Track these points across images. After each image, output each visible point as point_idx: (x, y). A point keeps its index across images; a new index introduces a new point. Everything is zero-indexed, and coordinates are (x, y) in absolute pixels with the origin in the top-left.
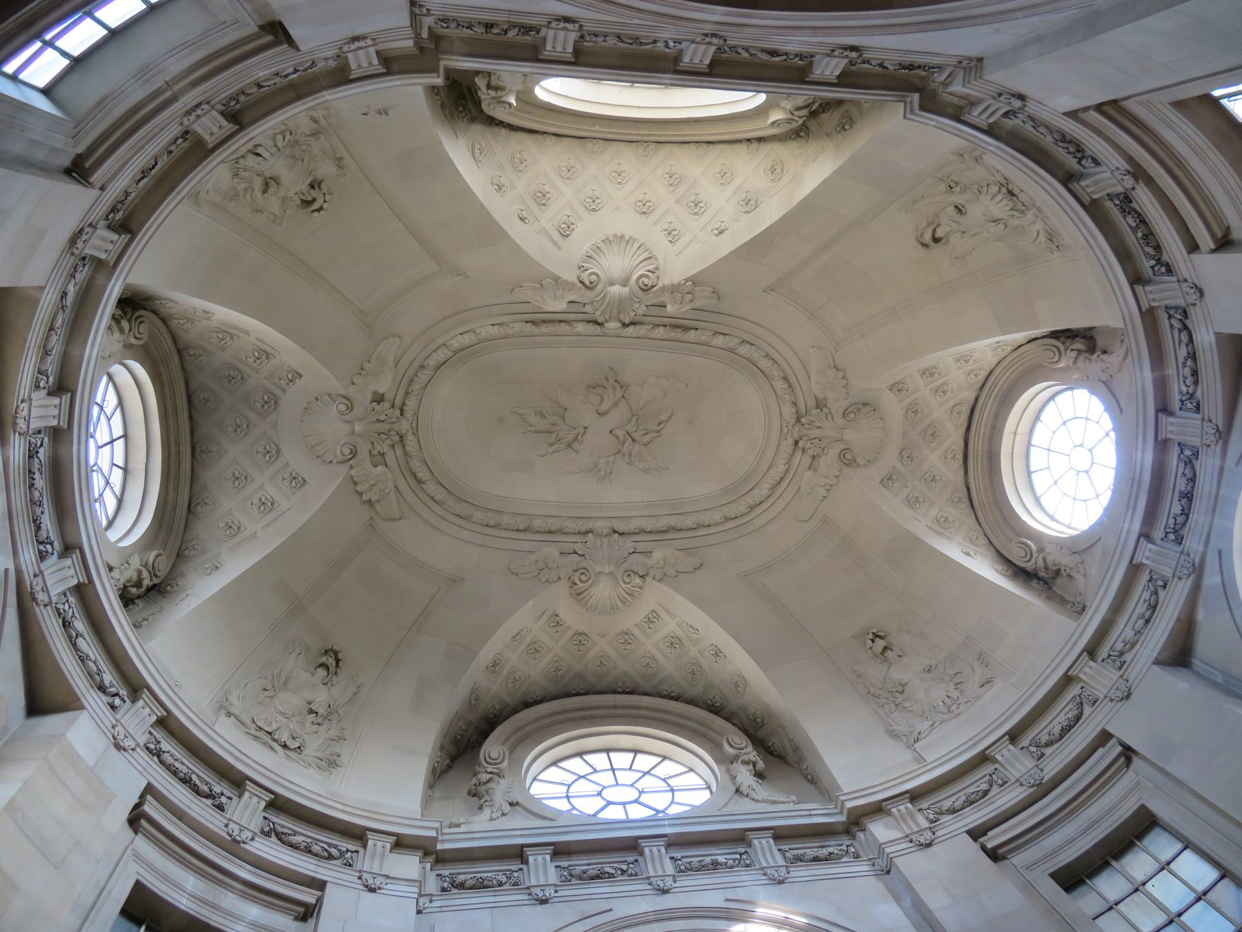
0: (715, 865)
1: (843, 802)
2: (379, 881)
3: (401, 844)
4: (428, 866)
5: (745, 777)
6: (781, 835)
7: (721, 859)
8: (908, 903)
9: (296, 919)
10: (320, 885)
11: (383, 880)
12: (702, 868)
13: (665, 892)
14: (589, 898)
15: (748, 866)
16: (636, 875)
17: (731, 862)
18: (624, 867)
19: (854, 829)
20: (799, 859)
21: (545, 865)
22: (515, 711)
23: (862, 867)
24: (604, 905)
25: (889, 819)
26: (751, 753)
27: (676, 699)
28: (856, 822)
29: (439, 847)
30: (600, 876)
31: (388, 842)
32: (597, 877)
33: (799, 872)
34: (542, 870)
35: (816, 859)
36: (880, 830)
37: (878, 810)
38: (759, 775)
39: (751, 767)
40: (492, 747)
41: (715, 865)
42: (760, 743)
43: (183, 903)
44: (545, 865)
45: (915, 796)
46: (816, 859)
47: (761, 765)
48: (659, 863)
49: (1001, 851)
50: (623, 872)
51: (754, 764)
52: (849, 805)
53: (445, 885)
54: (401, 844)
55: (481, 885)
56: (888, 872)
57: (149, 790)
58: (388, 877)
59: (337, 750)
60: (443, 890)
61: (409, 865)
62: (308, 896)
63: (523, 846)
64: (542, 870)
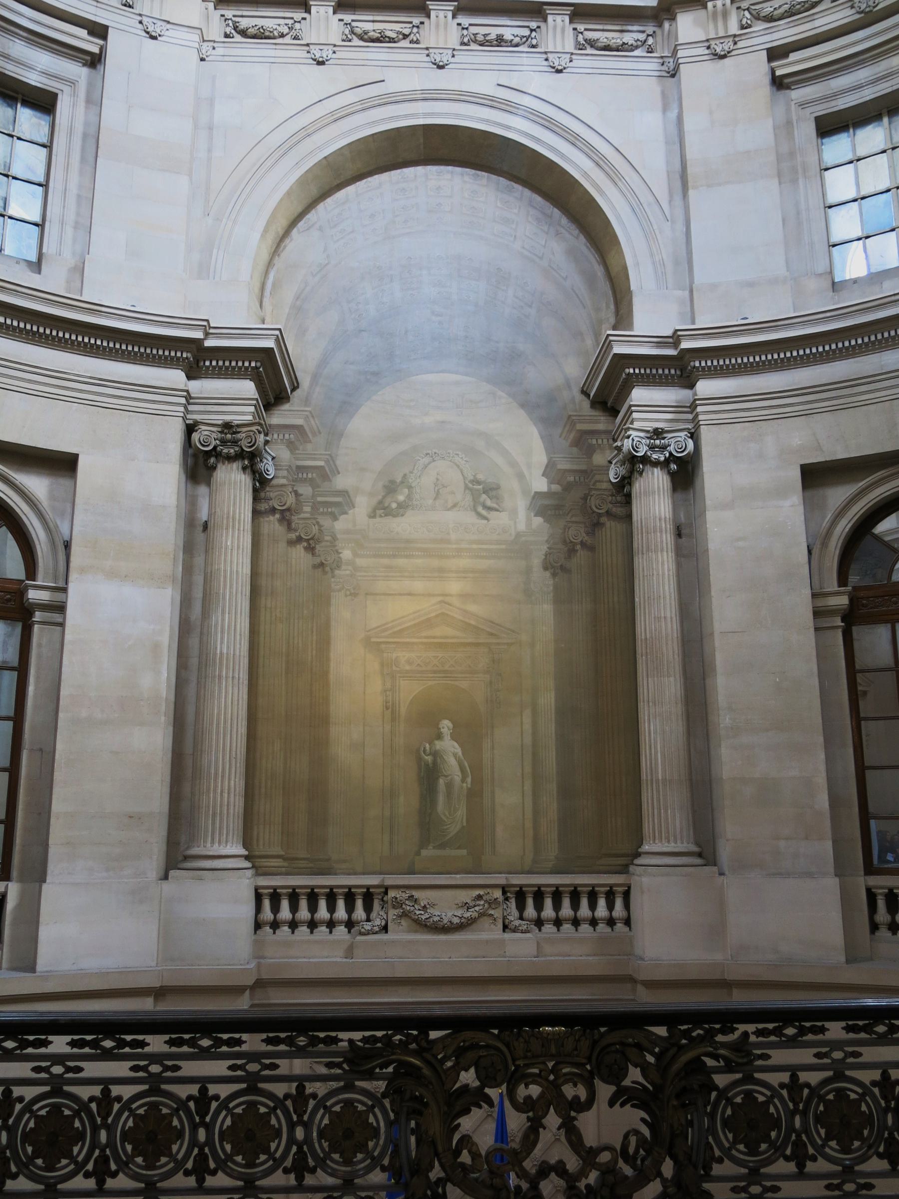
0: (500, 41)
7: (508, 33)
12: (485, 43)
15: (533, 46)
16: (417, 42)
17: (517, 40)
18: (406, 31)
20: (592, 43)
23: (652, 65)
30: (381, 39)
33: (586, 62)
35: (607, 48)
41: (500, 41)
46: (607, 48)
50: (405, 36)
62: (92, 46)
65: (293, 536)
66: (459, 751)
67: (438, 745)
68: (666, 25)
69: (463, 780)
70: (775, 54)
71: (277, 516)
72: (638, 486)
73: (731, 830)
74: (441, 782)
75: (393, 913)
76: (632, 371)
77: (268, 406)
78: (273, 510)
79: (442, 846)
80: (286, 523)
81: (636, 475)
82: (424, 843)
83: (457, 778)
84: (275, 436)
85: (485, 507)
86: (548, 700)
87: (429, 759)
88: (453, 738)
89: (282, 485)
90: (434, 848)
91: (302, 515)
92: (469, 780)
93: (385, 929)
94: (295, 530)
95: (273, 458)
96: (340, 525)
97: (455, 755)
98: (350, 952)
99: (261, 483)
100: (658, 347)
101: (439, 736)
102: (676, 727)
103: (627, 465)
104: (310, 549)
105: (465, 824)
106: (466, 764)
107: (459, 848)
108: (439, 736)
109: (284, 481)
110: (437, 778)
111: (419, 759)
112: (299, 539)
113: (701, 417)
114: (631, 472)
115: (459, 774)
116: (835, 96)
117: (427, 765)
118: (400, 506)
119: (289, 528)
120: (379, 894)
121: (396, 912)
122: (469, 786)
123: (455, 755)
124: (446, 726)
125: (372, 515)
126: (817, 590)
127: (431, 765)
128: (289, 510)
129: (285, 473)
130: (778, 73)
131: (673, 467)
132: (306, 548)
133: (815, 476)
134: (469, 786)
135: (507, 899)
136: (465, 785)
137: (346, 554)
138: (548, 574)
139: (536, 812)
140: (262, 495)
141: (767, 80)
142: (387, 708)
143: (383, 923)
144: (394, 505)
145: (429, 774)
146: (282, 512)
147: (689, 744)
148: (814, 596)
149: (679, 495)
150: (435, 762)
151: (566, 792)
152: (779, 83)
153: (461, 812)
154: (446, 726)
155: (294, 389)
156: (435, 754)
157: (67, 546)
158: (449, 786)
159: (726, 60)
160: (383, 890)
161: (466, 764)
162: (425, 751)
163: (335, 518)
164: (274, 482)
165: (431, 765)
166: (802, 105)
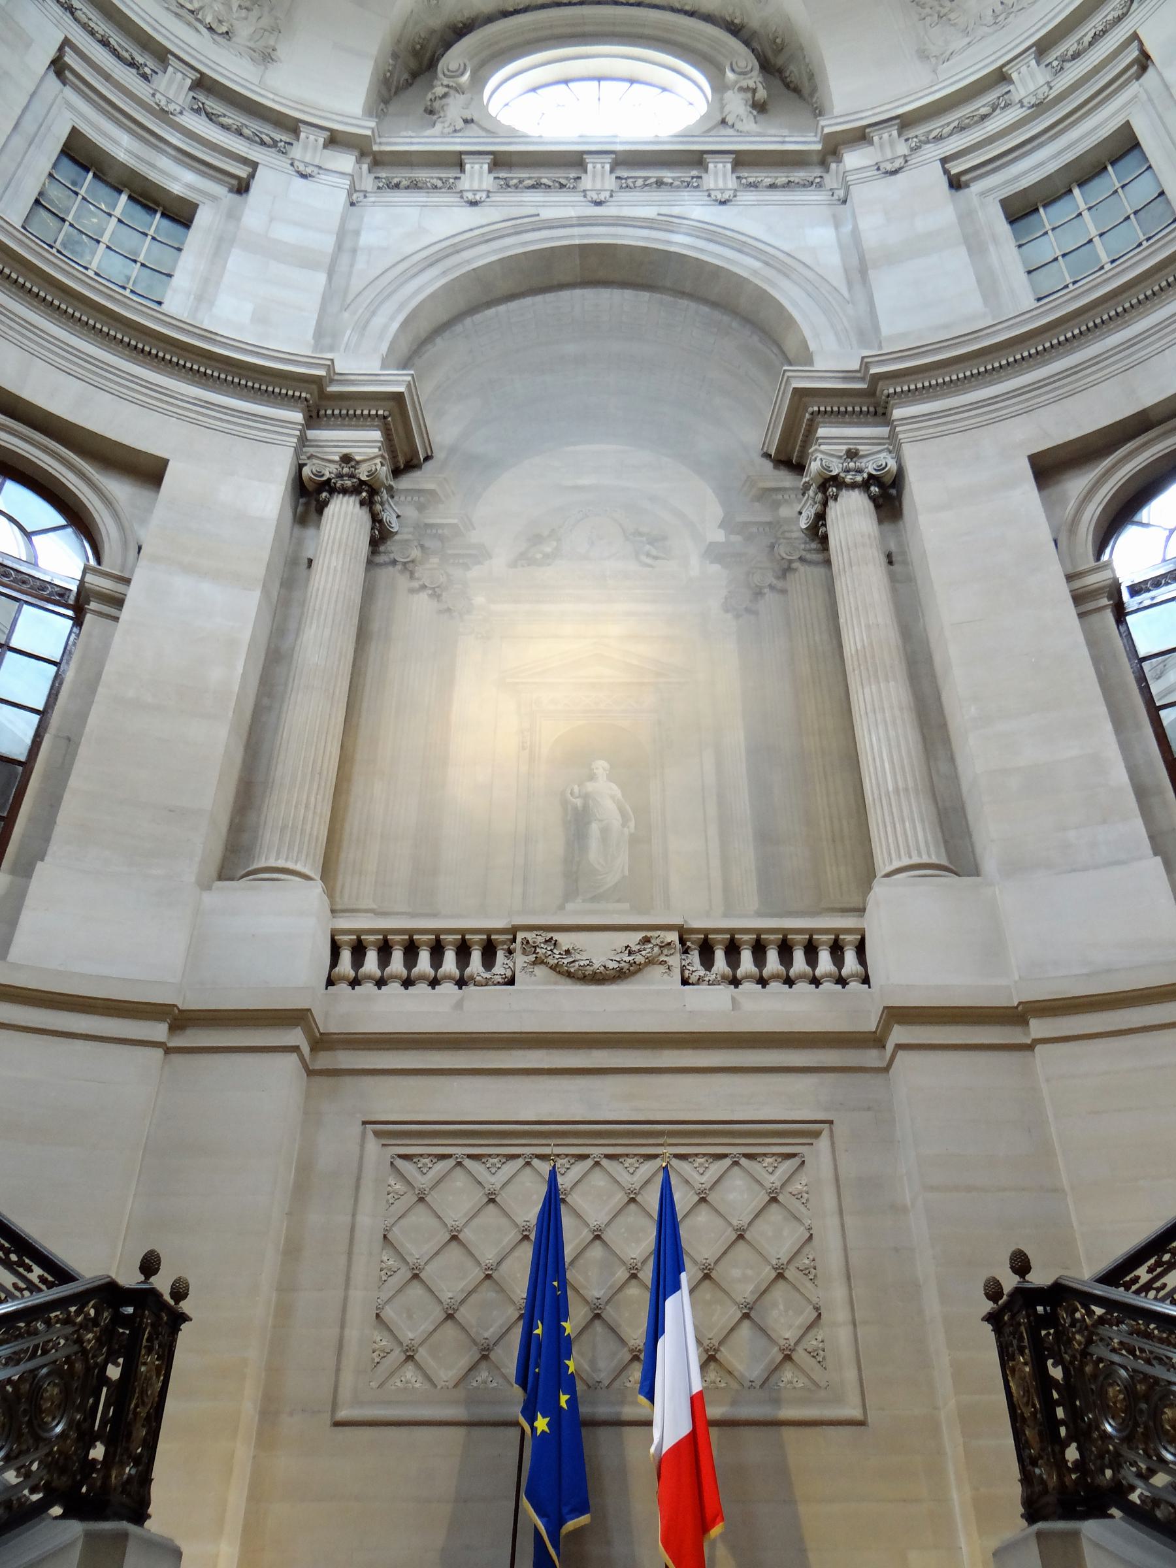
1: (823, 127)
2: (309, 170)
3: (335, 140)
4: (365, 167)
5: (737, 105)
6: (742, 160)
8: (847, 228)
9: (231, 191)
10: (255, 165)
11: (316, 170)
13: (598, 203)
14: (520, 204)
19: (830, 159)
21: (481, 174)
22: (490, 19)
24: (533, 211)
25: (871, 149)
26: (755, 79)
27: (691, 14)
28: (832, 149)
29: (375, 148)
31: (322, 138)
32: (533, 187)
34: (477, 176)
36: (853, 159)
37: (860, 136)
38: (760, 108)
39: (749, 95)
40: (453, 58)
42: (767, 67)
43: (121, 156)
44: (481, 174)
45: (905, 122)
47: (762, 94)
48: (598, 178)
49: (963, 178)
51: (754, 91)
52: (826, 130)
53: (381, 185)
54: (335, 140)
55: (415, 186)
56: (845, 202)
57: (66, 42)
58: (320, 168)
59: (272, 42)
60: (379, 188)
61: (345, 161)
63: (461, 153)
64: (477, 176)
65: (416, 584)
66: (618, 793)
67: (590, 787)
68: (833, 166)
69: (624, 825)
70: (944, 161)
71: (399, 567)
72: (834, 511)
73: (991, 832)
74: (595, 828)
75: (521, 960)
76: (816, 409)
77: (397, 472)
78: (394, 562)
79: (594, 899)
80: (408, 574)
81: (831, 503)
82: (571, 893)
83: (616, 821)
84: (402, 498)
85: (648, 555)
86: (736, 739)
87: (579, 802)
88: (610, 778)
89: (407, 540)
90: (584, 901)
91: (428, 566)
92: (632, 824)
93: (511, 982)
94: (418, 579)
95: (398, 517)
96: (475, 572)
97: (613, 797)
98: (459, 1005)
99: (380, 536)
100: (843, 383)
101: (592, 777)
102: (906, 735)
103: (820, 496)
104: (436, 595)
105: (627, 873)
106: (628, 807)
107: (618, 901)
108: (592, 777)
109: (410, 537)
110: (589, 823)
111: (564, 803)
112: (424, 587)
113: (900, 436)
114: (825, 504)
115: (619, 817)
116: (1017, 178)
117: (575, 808)
118: (546, 556)
119: (412, 576)
120: (504, 943)
121: (526, 959)
122: (633, 831)
123: (613, 797)
124: (601, 766)
125: (513, 564)
126: (1071, 571)
127: (580, 809)
128: (413, 561)
129: (411, 529)
130: (953, 172)
131: (874, 489)
132: (430, 596)
133: (1048, 468)
134: (633, 831)
135: (686, 952)
136: (626, 830)
137: (479, 600)
138: (729, 616)
139: (725, 862)
140: (382, 548)
141: (944, 182)
142: (524, 748)
143: (509, 974)
144: (539, 556)
145: (578, 822)
146: (405, 564)
147: (929, 769)
148: (1070, 578)
149: (887, 527)
150: (585, 807)
151: (765, 837)
152: (956, 183)
153: (622, 861)
154: (601, 766)
155: (427, 458)
156: (586, 797)
157: (140, 548)
158: (605, 831)
159: (899, 176)
160: (511, 937)
161: (628, 807)
162: (572, 794)
163: (467, 567)
164: (397, 537)
165: (580, 809)
166: (983, 194)
